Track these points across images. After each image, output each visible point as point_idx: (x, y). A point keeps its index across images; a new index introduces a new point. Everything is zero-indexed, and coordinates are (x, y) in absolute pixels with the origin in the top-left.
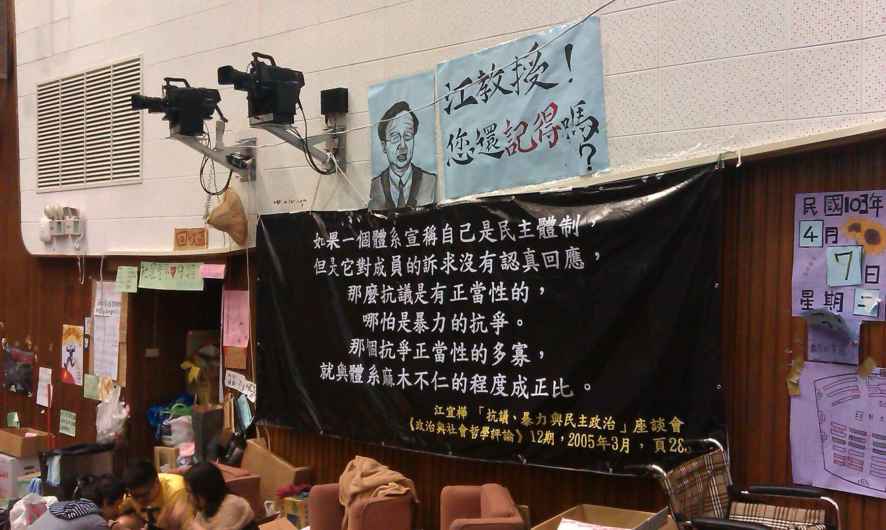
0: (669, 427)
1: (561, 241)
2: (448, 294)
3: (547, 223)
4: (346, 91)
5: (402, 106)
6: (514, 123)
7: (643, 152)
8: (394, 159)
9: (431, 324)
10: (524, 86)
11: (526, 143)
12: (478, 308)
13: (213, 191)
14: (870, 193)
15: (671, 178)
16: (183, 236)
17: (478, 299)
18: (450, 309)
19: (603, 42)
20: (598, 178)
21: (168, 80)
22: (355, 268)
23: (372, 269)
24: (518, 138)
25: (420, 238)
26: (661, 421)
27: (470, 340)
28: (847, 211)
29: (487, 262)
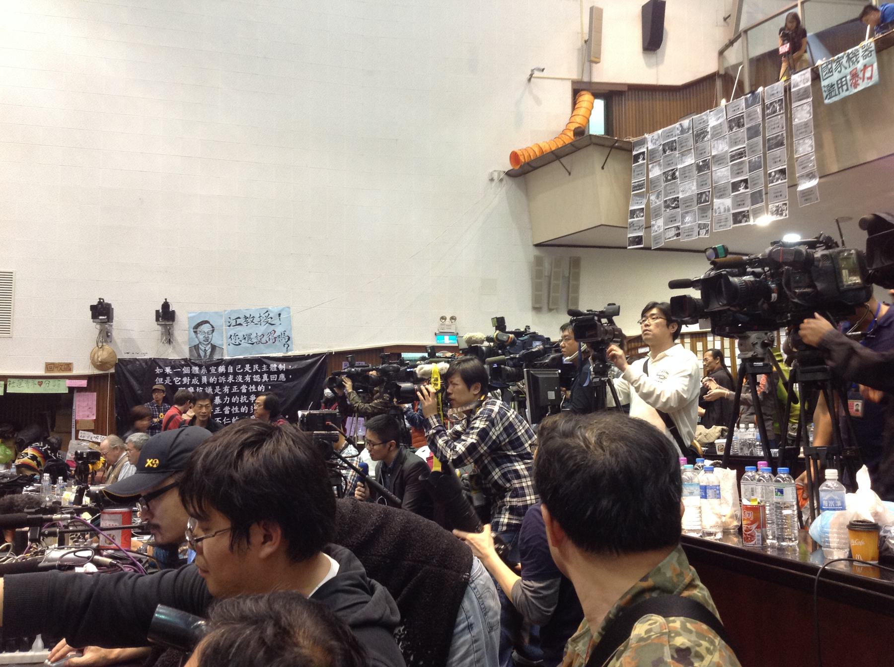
1: (278, 372)
2: (230, 389)
3: (274, 366)
5: (207, 322)
6: (259, 334)
7: (304, 348)
8: (201, 340)
9: (223, 400)
10: (263, 324)
11: (263, 340)
12: (244, 394)
15: (314, 355)
16: (49, 366)
17: (244, 391)
18: (231, 395)
20: (290, 354)
22: (181, 381)
23: (191, 381)
25: (216, 370)
27: (240, 405)
29: (248, 378)
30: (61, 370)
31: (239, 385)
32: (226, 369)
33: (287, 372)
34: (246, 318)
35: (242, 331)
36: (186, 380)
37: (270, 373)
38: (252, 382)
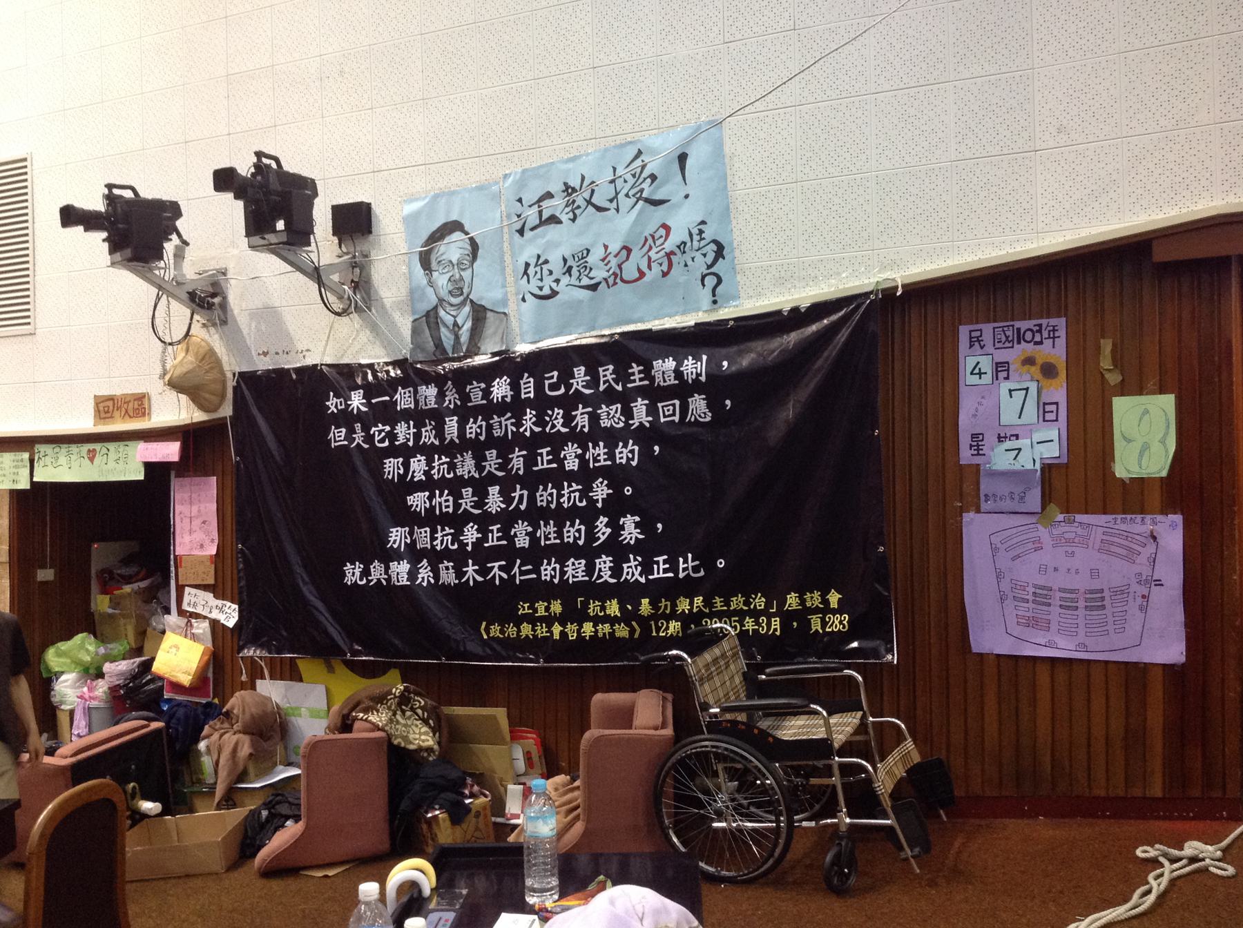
0: (826, 602)
1: (683, 389)
2: (530, 461)
3: (665, 367)
4: (367, 207)
5: (454, 226)
6: (614, 247)
7: (781, 282)
8: (444, 293)
9: (508, 500)
10: (625, 203)
11: (630, 271)
12: (571, 477)
13: (168, 340)
14: (1044, 322)
15: (820, 309)
16: (106, 406)
17: (572, 464)
18: (533, 480)
19: (727, 150)
20: (727, 312)
21: (110, 187)
22: (392, 436)
23: (418, 436)
24: (620, 266)
25: (487, 393)
26: (817, 594)
27: (561, 516)
28: (1019, 343)
29: (581, 418)
30: (128, 415)
31: (557, 443)
32: (515, 386)
33: (713, 387)
34: (568, 190)
35: (559, 243)
36: (404, 432)
37: (655, 394)
38: (597, 433)
